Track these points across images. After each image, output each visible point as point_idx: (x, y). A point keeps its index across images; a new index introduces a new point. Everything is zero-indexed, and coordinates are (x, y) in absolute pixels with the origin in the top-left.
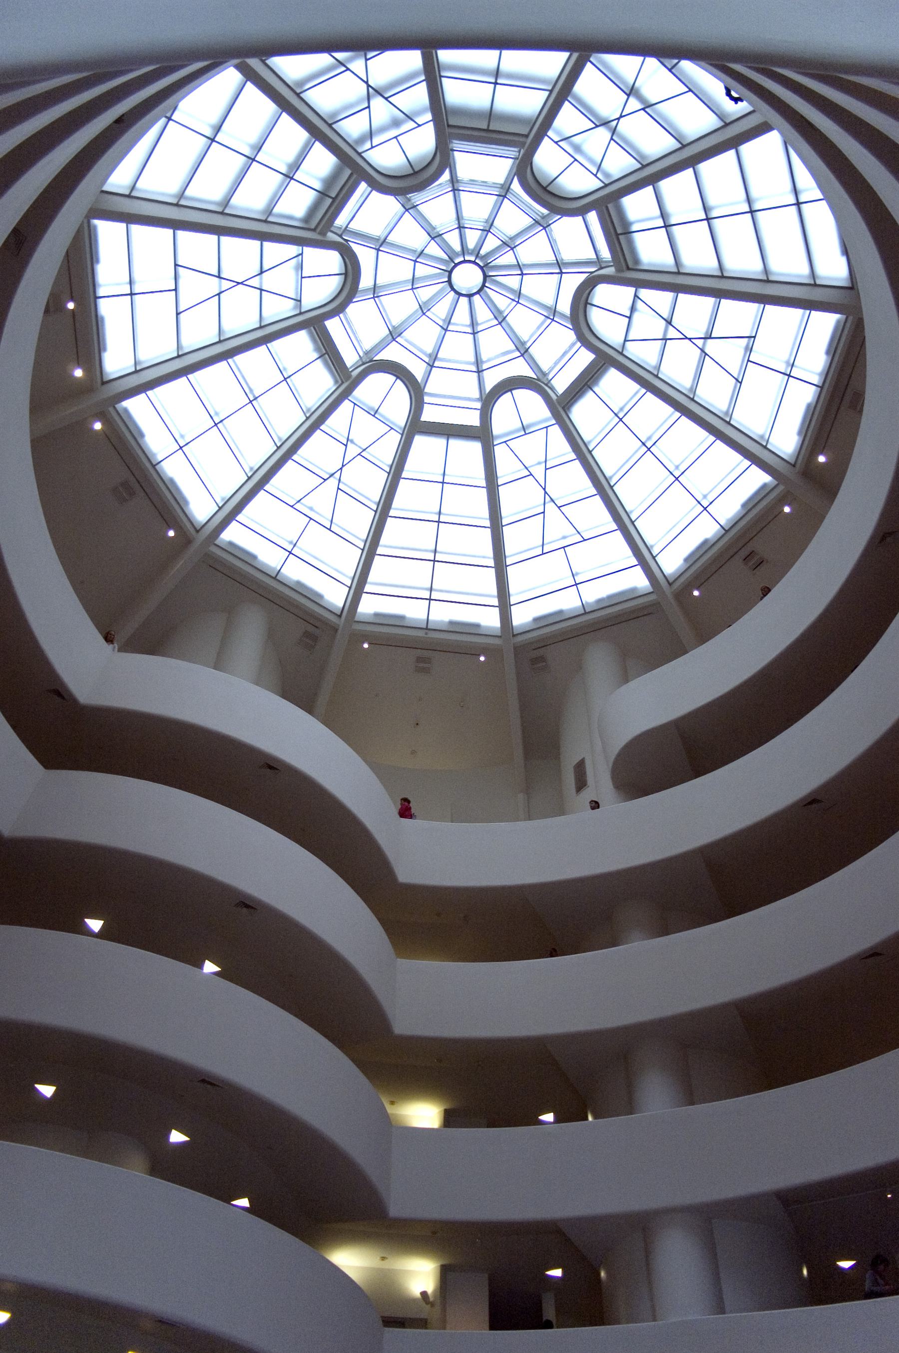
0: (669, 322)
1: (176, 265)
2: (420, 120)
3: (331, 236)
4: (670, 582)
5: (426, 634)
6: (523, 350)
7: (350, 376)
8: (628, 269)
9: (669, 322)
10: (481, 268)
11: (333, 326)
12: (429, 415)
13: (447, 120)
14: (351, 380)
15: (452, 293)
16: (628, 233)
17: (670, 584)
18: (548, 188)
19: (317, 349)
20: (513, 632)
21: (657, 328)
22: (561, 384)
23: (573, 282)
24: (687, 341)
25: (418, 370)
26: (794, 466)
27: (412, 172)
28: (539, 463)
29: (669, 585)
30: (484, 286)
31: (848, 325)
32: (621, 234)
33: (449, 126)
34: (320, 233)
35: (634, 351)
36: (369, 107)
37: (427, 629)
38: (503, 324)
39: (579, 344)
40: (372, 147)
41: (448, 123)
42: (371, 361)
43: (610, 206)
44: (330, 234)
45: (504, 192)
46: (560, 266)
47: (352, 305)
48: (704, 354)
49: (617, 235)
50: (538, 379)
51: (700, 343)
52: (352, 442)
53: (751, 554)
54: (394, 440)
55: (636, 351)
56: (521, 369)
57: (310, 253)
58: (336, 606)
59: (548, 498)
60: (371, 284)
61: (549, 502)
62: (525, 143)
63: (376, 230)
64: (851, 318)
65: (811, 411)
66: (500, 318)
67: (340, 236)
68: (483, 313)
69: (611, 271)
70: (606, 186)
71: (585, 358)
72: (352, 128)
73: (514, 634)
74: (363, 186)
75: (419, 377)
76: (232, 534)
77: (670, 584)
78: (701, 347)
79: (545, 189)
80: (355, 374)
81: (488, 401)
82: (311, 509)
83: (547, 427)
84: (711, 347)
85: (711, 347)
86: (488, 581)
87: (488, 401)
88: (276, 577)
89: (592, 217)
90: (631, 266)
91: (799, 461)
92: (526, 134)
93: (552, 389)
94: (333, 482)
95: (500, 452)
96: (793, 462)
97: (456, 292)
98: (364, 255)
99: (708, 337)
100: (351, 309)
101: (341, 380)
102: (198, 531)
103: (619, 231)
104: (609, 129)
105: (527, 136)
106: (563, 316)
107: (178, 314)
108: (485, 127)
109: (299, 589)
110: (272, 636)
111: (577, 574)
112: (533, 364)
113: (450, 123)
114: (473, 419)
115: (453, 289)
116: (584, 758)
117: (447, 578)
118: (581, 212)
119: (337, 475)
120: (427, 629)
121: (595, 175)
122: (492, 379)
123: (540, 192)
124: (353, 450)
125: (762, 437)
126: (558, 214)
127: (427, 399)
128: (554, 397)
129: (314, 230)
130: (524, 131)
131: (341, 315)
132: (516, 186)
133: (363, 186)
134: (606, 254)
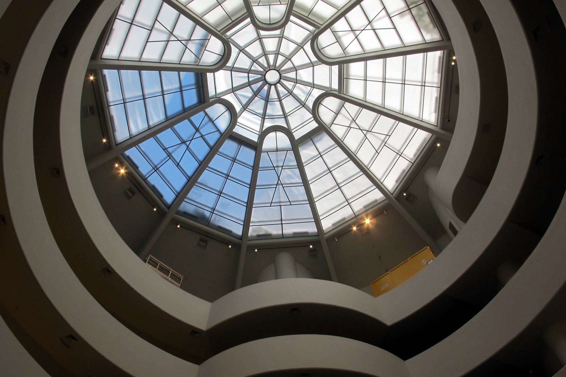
0: (352, 30)
1: (165, 149)
3: (211, 100)
4: (436, 125)
5: (357, 218)
6: (313, 86)
9: (352, 30)
10: (274, 69)
12: (297, 135)
13: (217, 31)
15: (267, 85)
17: (437, 126)
20: (391, 193)
21: (351, 36)
24: (363, 31)
25: (282, 123)
26: (443, 40)
27: (221, 57)
29: (436, 127)
30: (280, 75)
32: (308, 16)
33: (219, 31)
36: (186, 47)
37: (356, 216)
38: (298, 82)
40: (200, 60)
41: (217, 31)
44: (210, 100)
50: (327, 91)
52: (278, 167)
56: (316, 93)
58: (315, 233)
59: (365, 132)
61: (367, 133)
67: (216, 98)
70: (288, 4)
72: (189, 58)
73: (392, 193)
76: (252, 232)
77: (437, 126)
78: (371, 29)
82: (280, 202)
86: (364, 181)
88: (283, 236)
93: (336, 91)
96: (442, 39)
100: (239, 120)
106: (315, 62)
107: (178, 165)
108: (231, 21)
109: (296, 235)
110: (296, 260)
111: (399, 151)
112: (319, 87)
113: (219, 30)
114: (314, 125)
116: (450, 224)
117: (349, 191)
119: (279, 182)
120: (356, 216)
121: (281, 4)
122: (310, 104)
128: (336, 93)
131: (237, 124)
132: (262, 33)
134: (311, 28)
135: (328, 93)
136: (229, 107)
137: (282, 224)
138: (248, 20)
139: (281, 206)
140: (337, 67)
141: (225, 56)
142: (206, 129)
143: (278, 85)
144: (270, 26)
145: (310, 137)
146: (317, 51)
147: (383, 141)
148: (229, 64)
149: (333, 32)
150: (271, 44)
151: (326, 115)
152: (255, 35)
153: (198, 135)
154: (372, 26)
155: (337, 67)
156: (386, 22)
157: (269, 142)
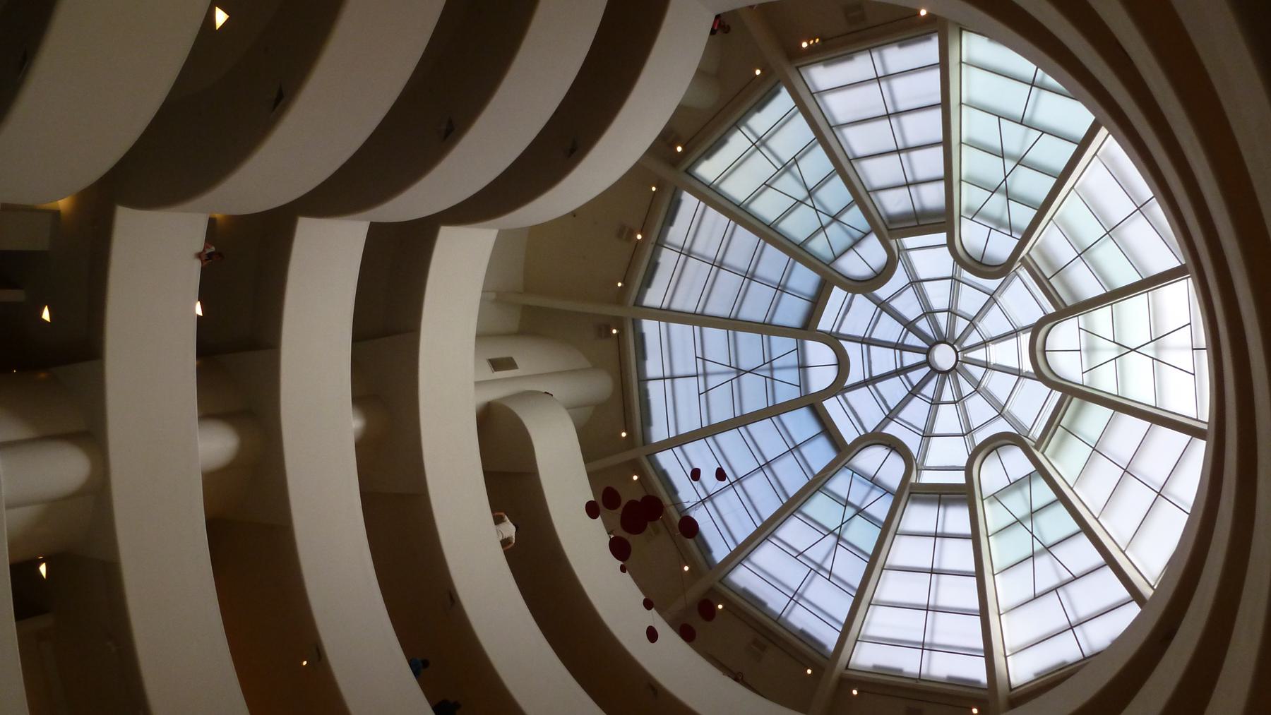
6: (871, 381)
7: (892, 239)
8: (910, 493)
14: (887, 236)
18: (995, 451)
22: (832, 406)
23: (912, 442)
28: (772, 375)
34: (1023, 257)
39: (862, 433)
42: (899, 258)
46: (927, 435)
47: (952, 260)
48: (826, 534)
49: (940, 494)
54: (828, 255)
56: (855, 375)
62: (1038, 451)
66: (902, 371)
68: (910, 358)
69: (913, 480)
71: (849, 434)
74: (1051, 309)
80: (893, 242)
83: (800, 386)
84: (831, 540)
85: (831, 540)
90: (912, 495)
92: (1045, 453)
94: (802, 194)
95: (790, 343)
99: (839, 537)
101: (891, 230)
102: (797, 68)
103: (942, 496)
104: (1025, 518)
105: (1043, 453)
118: (968, 469)
119: (809, 202)
122: (853, 350)
124: (825, 219)
125: (749, 560)
126: (972, 452)
127: (850, 294)
129: (1028, 254)
134: (928, 478)
135: (838, 388)
137: (664, 378)
139: (779, 170)
140: (849, 440)
145: (817, 303)
146: (895, 446)
147: (705, 374)
149: (887, 491)
150: (979, 409)
152: (1014, 408)
154: (835, 534)
155: (849, 440)
156: (817, 554)
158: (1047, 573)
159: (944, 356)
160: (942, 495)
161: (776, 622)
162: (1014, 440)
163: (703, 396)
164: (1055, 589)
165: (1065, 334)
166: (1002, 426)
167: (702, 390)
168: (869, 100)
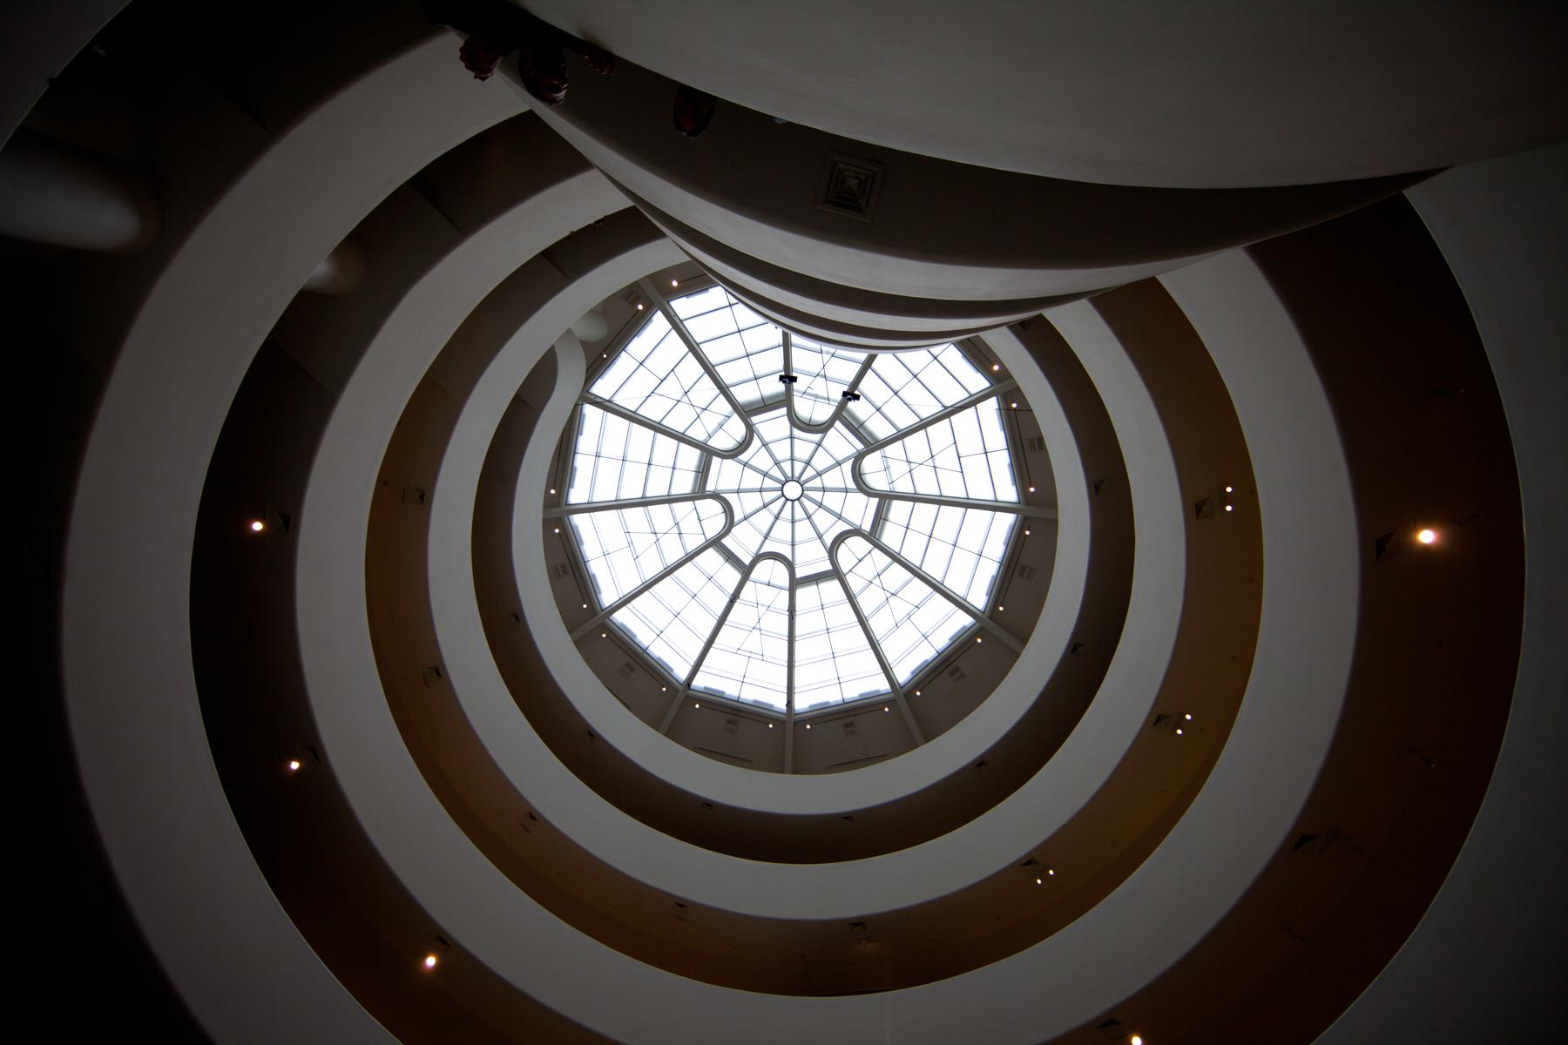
2: (831, 403)
11: (716, 460)
12: (726, 541)
16: (886, 520)
19: (699, 466)
23: (842, 527)
31: (975, 627)
35: (850, 579)
43: (887, 501)
45: (839, 464)
47: (731, 460)
51: (888, 595)
53: (851, 724)
54: (701, 541)
55: (851, 580)
57: (736, 418)
60: (746, 460)
63: (767, 439)
64: (978, 624)
65: (926, 665)
74: (784, 411)
75: (737, 519)
79: (860, 475)
81: (759, 558)
82: (632, 543)
87: (759, 558)
89: (874, 501)
91: (906, 687)
95: (748, 585)
97: (783, 493)
98: (756, 442)
114: (747, 560)
115: (782, 490)
122: (769, 547)
123: (857, 473)
130: (872, 442)
133: (784, 411)
134: (867, 527)
136: (744, 445)
138: (860, 446)
141: (809, 427)
142: (710, 420)
143: (797, 503)
144: (857, 475)
145: (731, 557)
148: (797, 432)
151: (764, 570)
153: (699, 411)
157: (710, 508)
158: (947, 459)
159: (792, 490)
160: (880, 518)
161: (940, 654)
162: (859, 458)
163: (765, 658)
164: (959, 458)
165: (803, 408)
166: (848, 466)
167: (761, 658)
168: (609, 469)
